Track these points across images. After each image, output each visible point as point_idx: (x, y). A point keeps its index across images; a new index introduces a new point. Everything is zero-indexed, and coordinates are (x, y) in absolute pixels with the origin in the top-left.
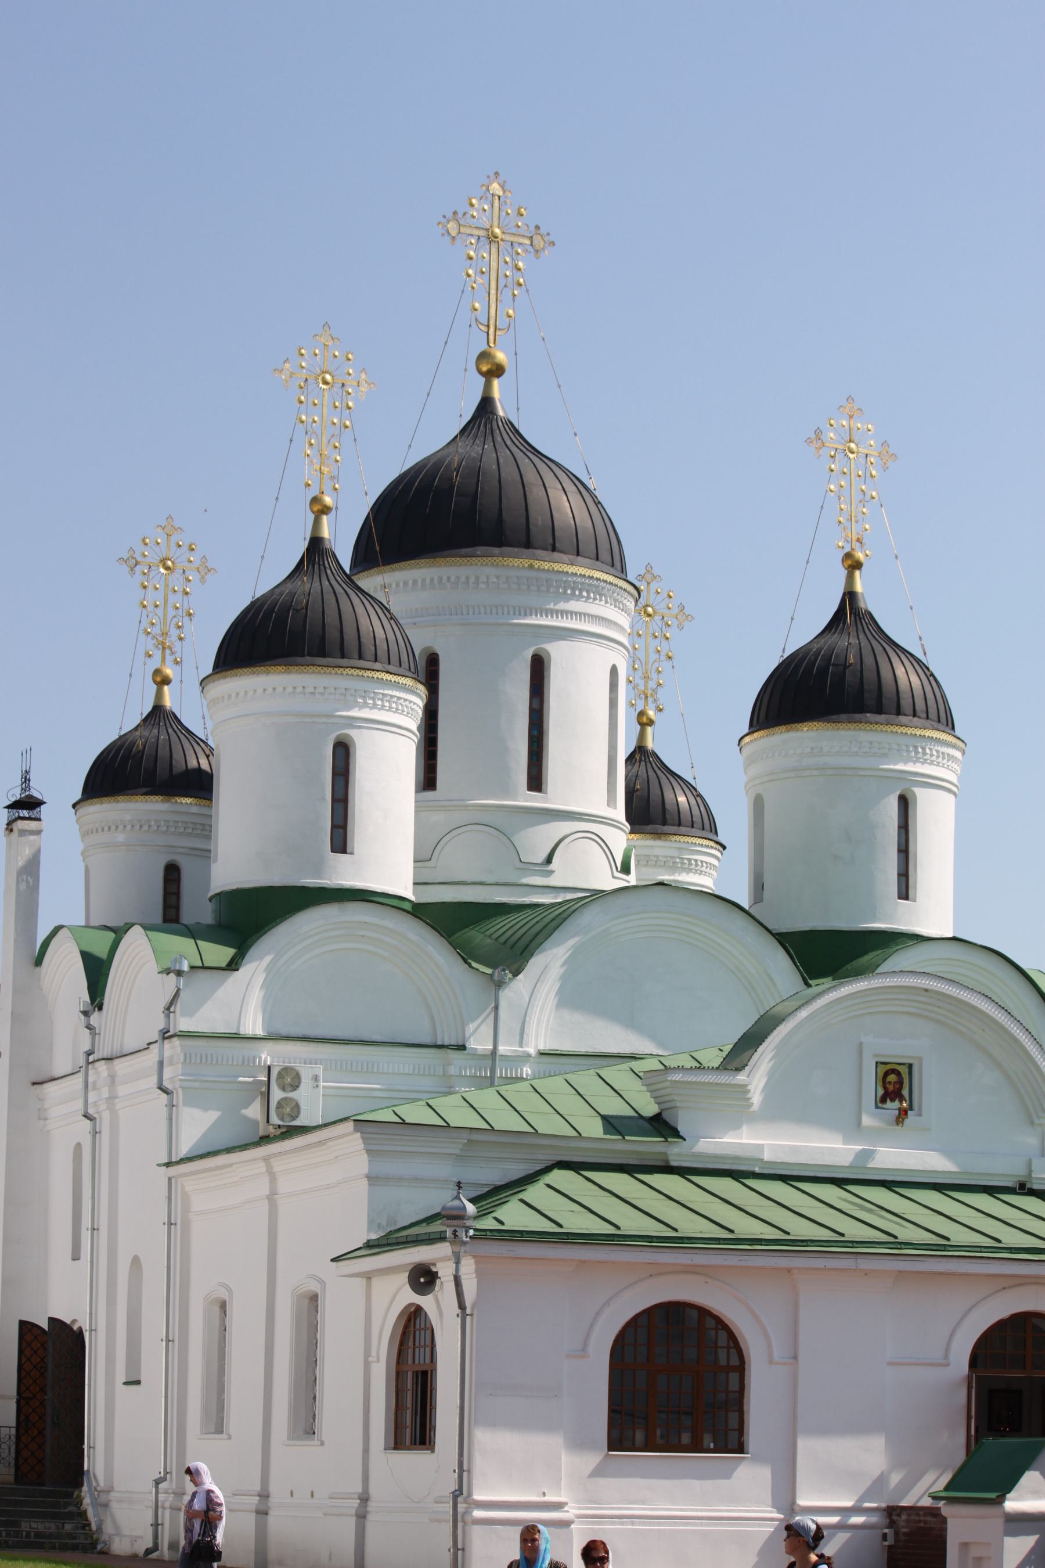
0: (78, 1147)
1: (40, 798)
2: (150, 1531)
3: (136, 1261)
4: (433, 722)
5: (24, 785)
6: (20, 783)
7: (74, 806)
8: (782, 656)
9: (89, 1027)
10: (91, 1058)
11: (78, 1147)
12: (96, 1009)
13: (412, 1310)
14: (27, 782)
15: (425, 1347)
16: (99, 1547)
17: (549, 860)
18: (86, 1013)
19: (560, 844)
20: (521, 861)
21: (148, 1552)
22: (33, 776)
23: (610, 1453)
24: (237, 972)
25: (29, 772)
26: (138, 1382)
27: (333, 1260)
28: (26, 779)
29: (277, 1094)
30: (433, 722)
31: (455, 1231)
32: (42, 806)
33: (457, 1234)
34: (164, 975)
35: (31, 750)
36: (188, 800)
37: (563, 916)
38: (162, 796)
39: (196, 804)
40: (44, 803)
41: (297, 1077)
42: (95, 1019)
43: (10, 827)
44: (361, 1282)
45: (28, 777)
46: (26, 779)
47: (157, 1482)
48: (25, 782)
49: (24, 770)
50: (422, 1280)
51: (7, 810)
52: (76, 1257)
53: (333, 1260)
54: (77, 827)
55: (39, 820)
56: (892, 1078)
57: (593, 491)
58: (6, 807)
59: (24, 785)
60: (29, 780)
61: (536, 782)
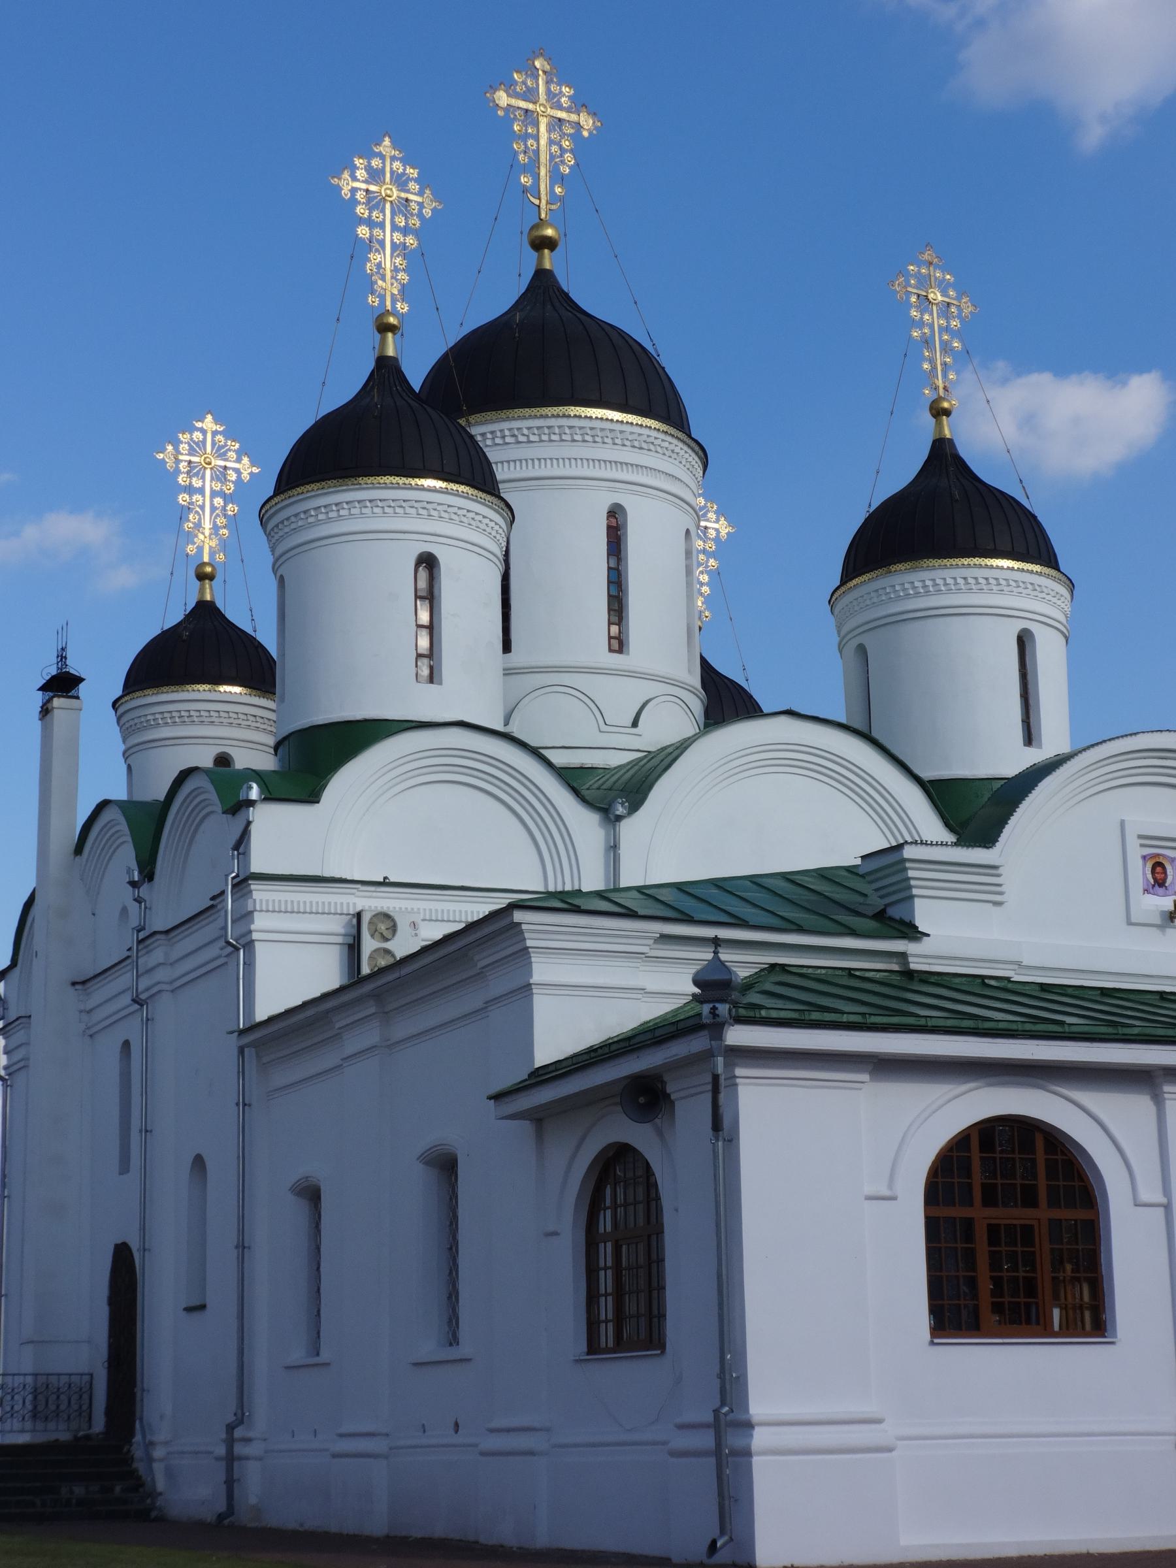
0: (126, 1044)
1: (77, 674)
2: (224, 1487)
3: (199, 1163)
4: (504, 583)
5: (60, 664)
6: (56, 662)
7: (115, 704)
8: (868, 511)
9: (138, 900)
10: (142, 935)
11: (126, 1044)
12: (146, 879)
13: (611, 1154)
14: (64, 660)
15: (635, 1203)
16: (153, 1514)
17: (635, 724)
18: (133, 884)
19: (644, 708)
20: (606, 724)
21: (221, 1517)
22: (69, 654)
23: (936, 1341)
24: (317, 805)
25: (66, 647)
26: (202, 1307)
27: (490, 1098)
28: (62, 657)
29: (369, 945)
30: (504, 583)
31: (714, 1008)
32: (81, 686)
33: (717, 1012)
34: (229, 816)
35: (67, 624)
36: (237, 689)
37: (684, 745)
38: (209, 684)
39: (246, 694)
40: (80, 680)
41: (394, 928)
42: (144, 891)
43: (45, 707)
44: (526, 1126)
45: (64, 655)
46: (62, 657)
47: (230, 1428)
48: (61, 660)
49: (60, 647)
50: (642, 1100)
51: (41, 692)
52: (124, 1168)
53: (490, 1098)
54: (118, 728)
55: (77, 698)
56: (1159, 869)
57: (657, 358)
58: (39, 690)
59: (60, 664)
60: (66, 658)
61: (619, 644)
